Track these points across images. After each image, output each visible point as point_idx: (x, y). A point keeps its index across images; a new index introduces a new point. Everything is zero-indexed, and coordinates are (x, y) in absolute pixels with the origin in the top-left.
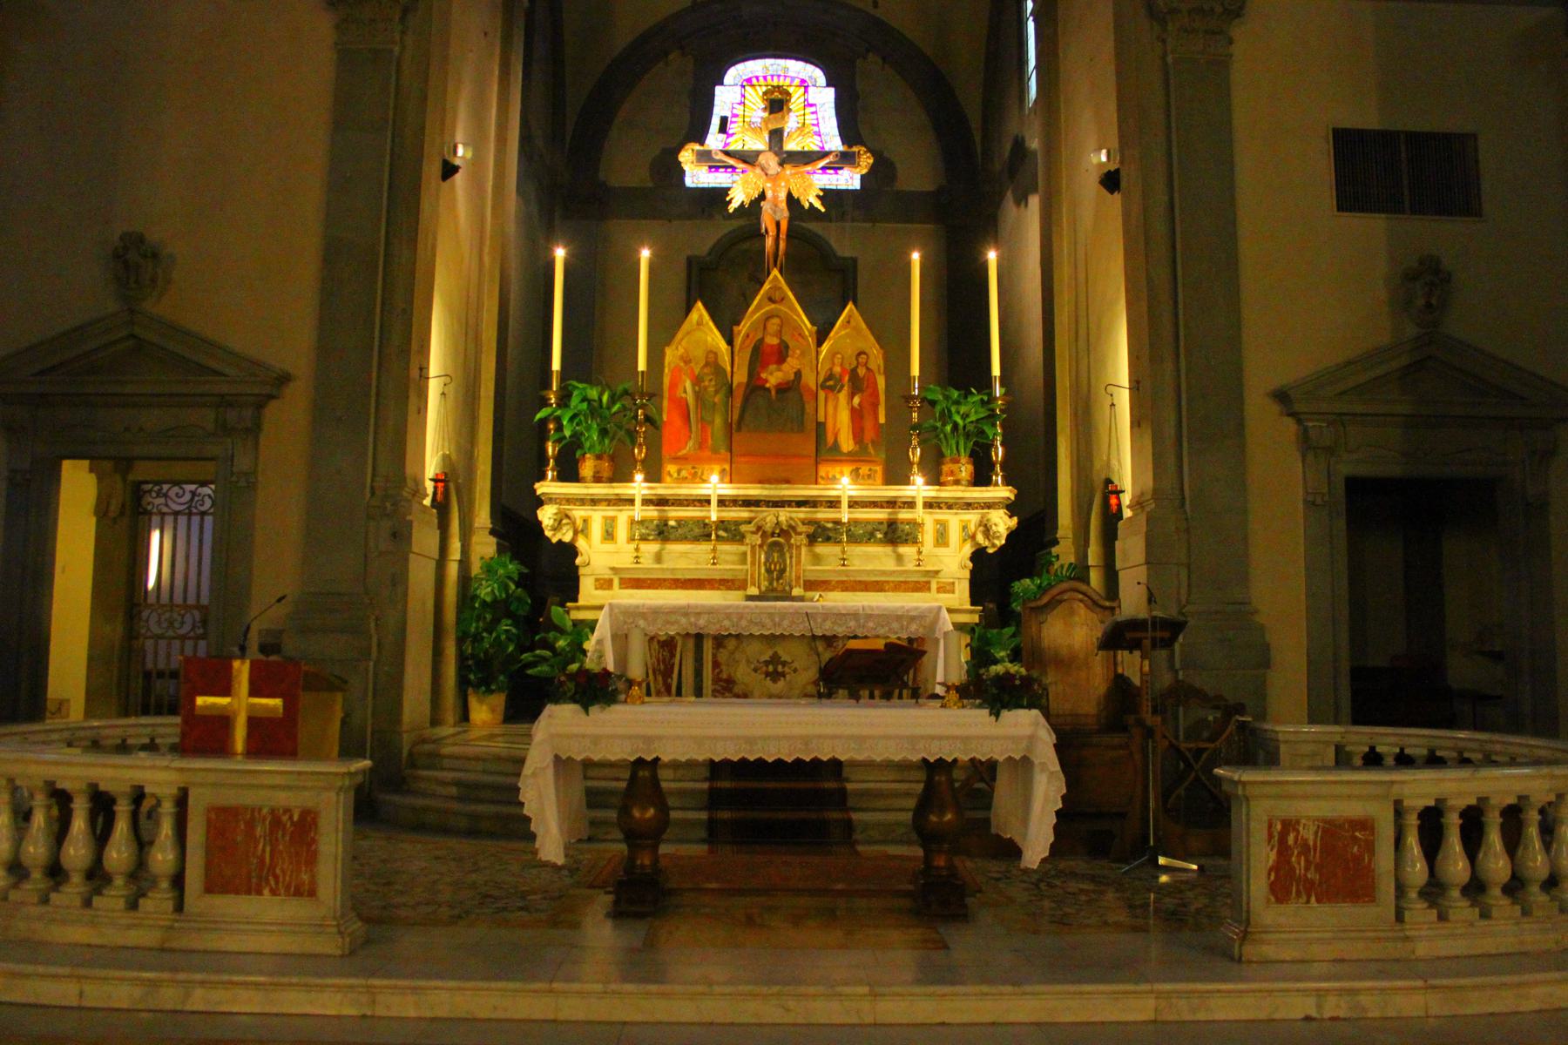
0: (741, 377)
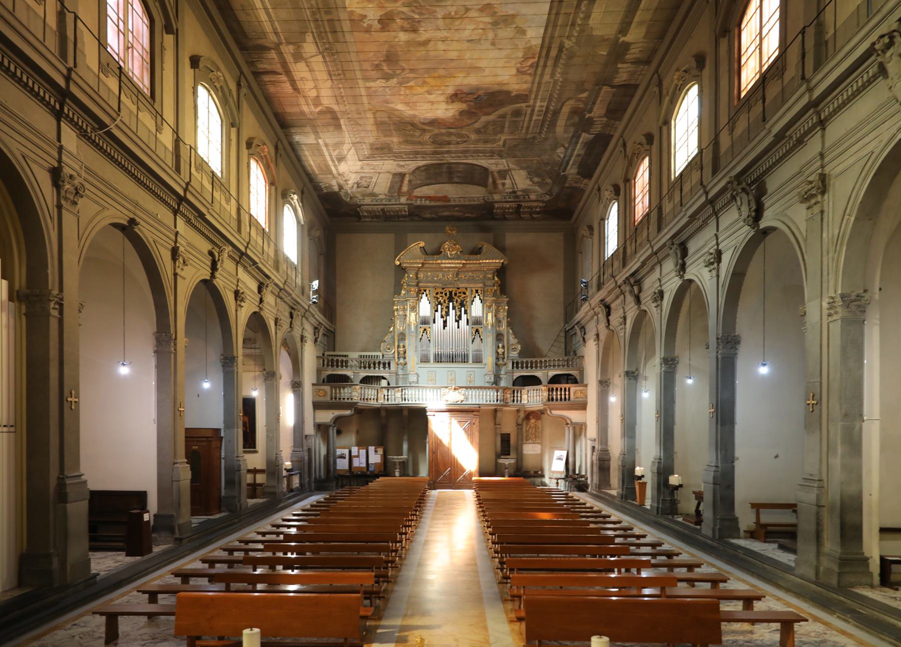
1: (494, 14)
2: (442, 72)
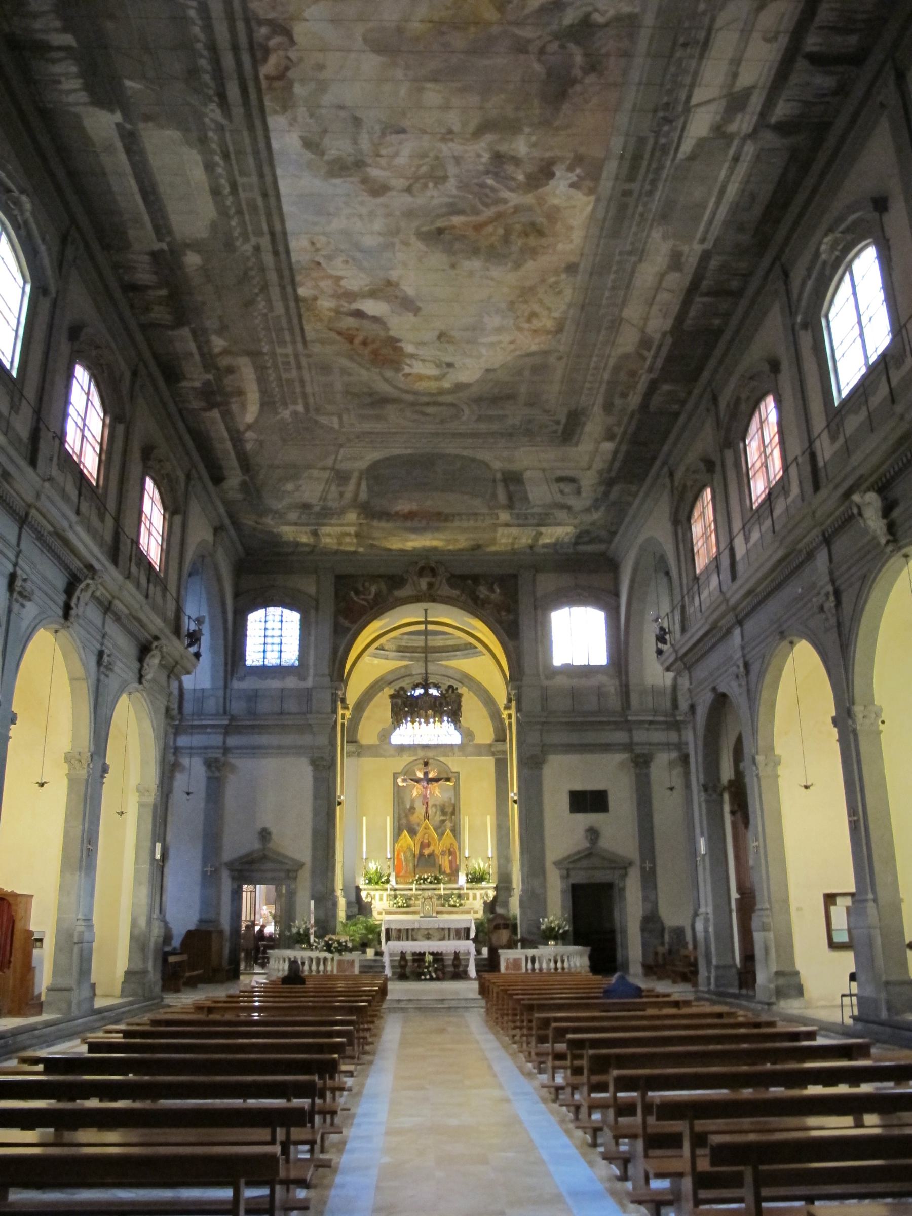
0: (417, 852)
2: (458, 41)
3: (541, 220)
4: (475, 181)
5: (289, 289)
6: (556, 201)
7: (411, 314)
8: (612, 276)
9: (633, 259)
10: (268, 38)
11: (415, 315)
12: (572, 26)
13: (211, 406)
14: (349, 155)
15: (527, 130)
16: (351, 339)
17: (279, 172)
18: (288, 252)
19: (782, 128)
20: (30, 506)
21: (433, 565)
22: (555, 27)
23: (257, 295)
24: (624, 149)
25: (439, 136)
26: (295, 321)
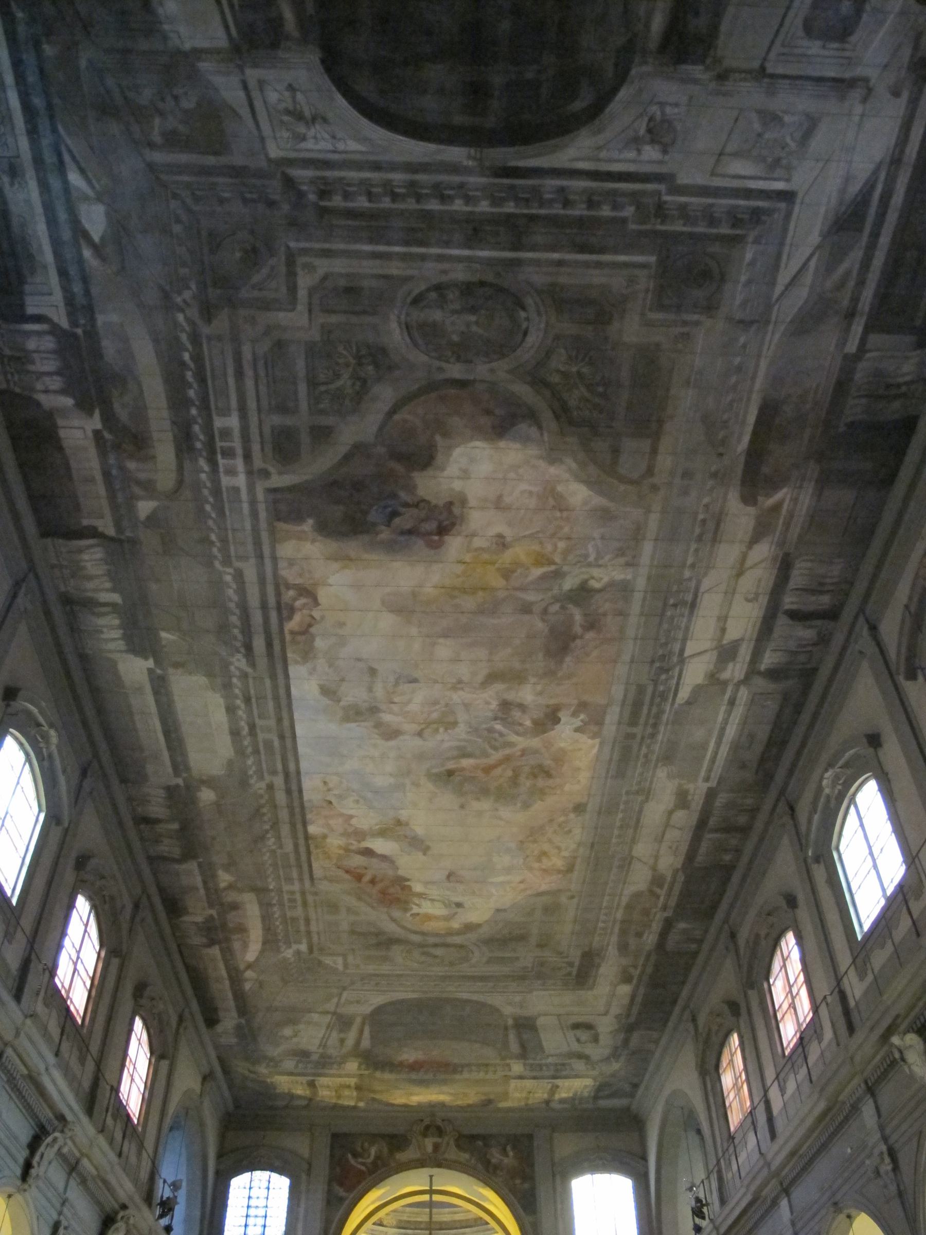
1: (378, 725)
2: (469, 603)
3: (548, 762)
4: (484, 726)
5: (299, 826)
6: (562, 745)
7: (420, 854)
8: (620, 815)
9: (640, 798)
10: (295, 599)
11: (425, 854)
12: (571, 590)
13: (212, 943)
14: (365, 702)
15: (533, 680)
16: (359, 878)
17: (296, 716)
18: (300, 791)
19: (774, 674)
20: (6, 1044)
21: (439, 1123)
22: (556, 591)
23: (267, 832)
24: (625, 696)
25: (450, 686)
26: (304, 858)
